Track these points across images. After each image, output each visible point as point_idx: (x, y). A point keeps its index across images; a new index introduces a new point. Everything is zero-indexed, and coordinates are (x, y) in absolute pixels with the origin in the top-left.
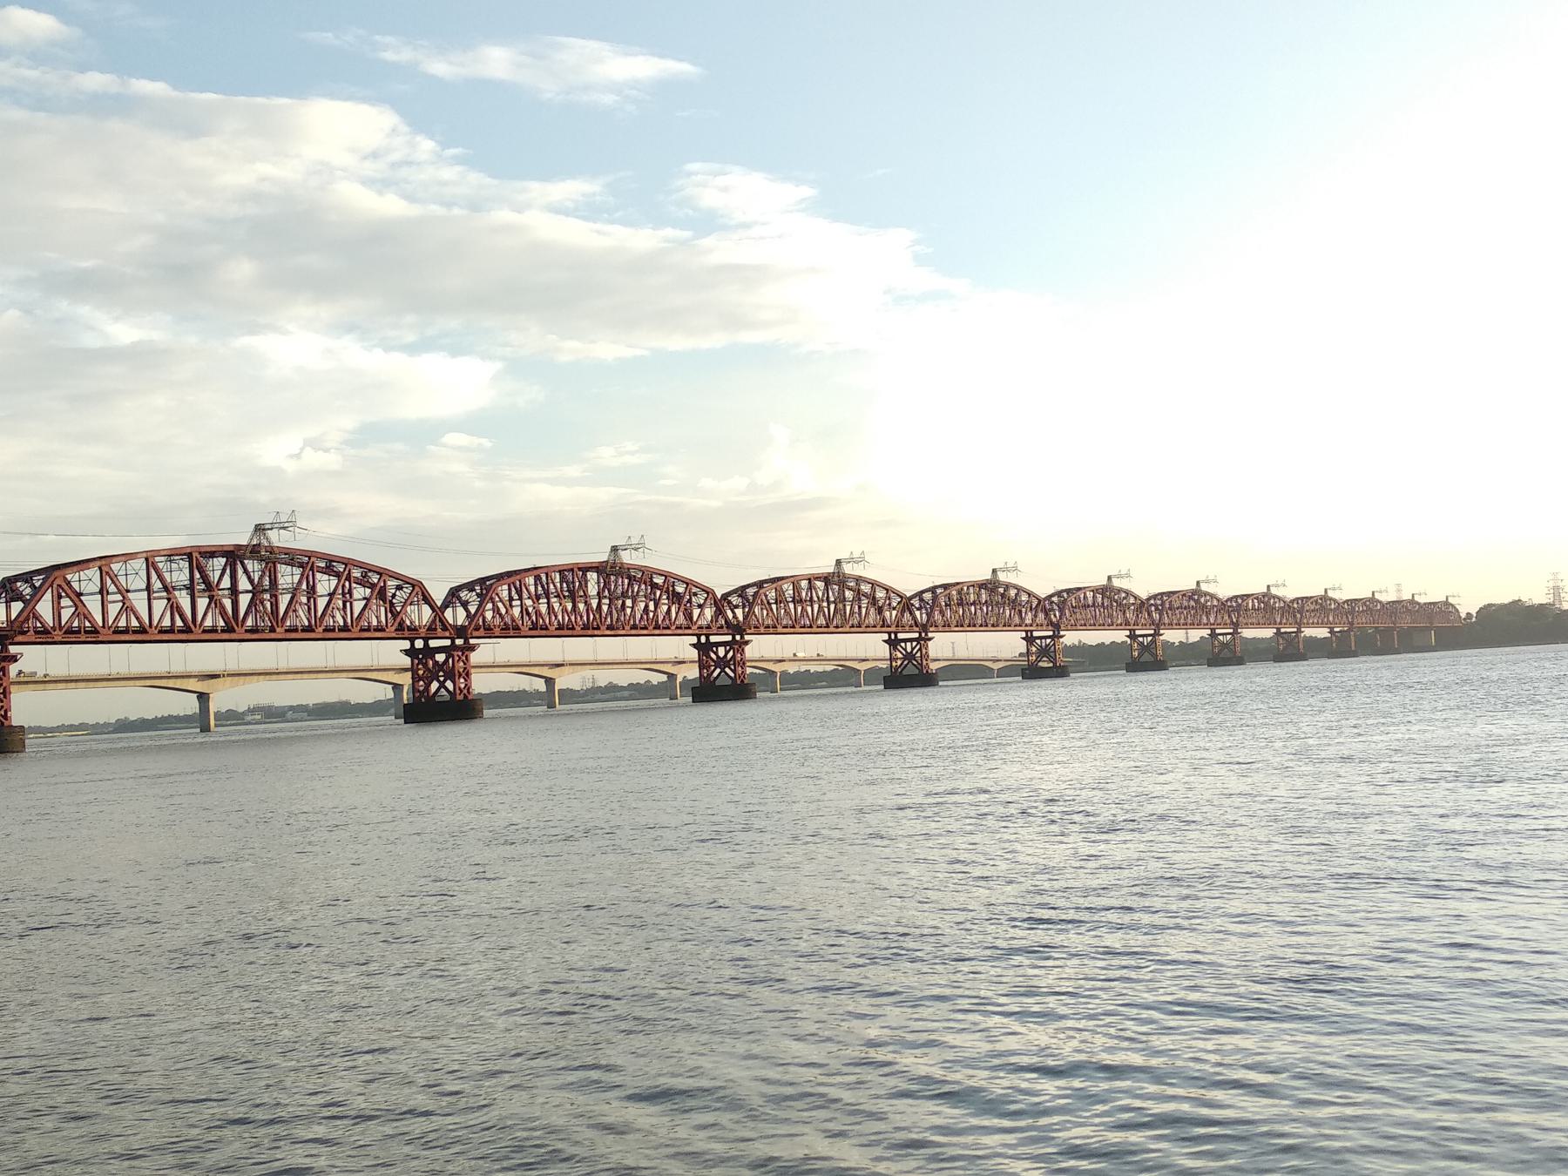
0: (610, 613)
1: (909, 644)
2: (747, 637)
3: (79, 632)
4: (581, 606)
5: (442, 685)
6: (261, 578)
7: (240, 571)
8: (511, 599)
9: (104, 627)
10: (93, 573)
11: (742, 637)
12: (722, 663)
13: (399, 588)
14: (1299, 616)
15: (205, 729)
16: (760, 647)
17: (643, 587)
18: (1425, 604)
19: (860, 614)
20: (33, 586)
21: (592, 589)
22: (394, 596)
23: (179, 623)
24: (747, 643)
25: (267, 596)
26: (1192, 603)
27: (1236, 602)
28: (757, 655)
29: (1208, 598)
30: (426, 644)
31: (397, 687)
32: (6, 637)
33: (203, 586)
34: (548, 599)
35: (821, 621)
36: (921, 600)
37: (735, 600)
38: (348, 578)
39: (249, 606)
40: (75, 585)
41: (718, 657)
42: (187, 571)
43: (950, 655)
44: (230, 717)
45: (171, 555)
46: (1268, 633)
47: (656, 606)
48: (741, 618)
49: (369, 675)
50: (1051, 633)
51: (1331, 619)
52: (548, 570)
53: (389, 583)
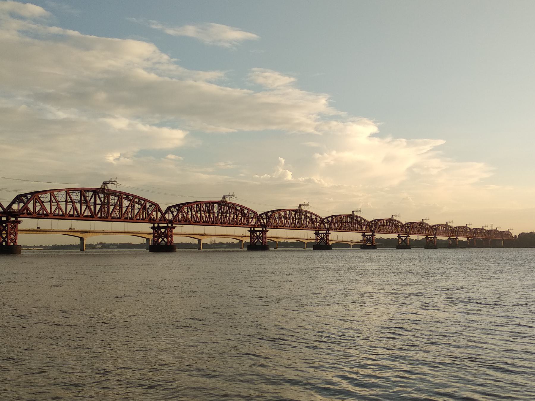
0: (221, 218)
1: (322, 235)
2: (267, 229)
3: (42, 215)
4: (212, 215)
5: (163, 239)
6: (104, 200)
7: (97, 197)
8: (188, 212)
9: (50, 213)
10: (48, 195)
11: (266, 229)
12: (258, 237)
13: (150, 206)
14: (457, 233)
15: (82, 250)
16: (272, 233)
17: (233, 210)
18: (501, 231)
19: (306, 223)
20: (27, 198)
21: (216, 210)
22: (149, 208)
23: (76, 213)
24: (267, 231)
25: (106, 206)
26: (420, 226)
27: (436, 227)
28: (270, 236)
29: (426, 225)
30: (158, 225)
31: (148, 239)
32: (17, 215)
33: (84, 202)
34: (201, 212)
35: (293, 225)
36: (328, 220)
37: (264, 216)
38: (134, 202)
39: (99, 209)
40: (42, 199)
42: (79, 196)
43: (336, 239)
44: (91, 246)
45: (75, 190)
46: (446, 238)
47: (237, 217)
48: (266, 223)
49: (138, 235)
50: (371, 234)
51: (468, 234)
52: (201, 203)
53: (147, 204)
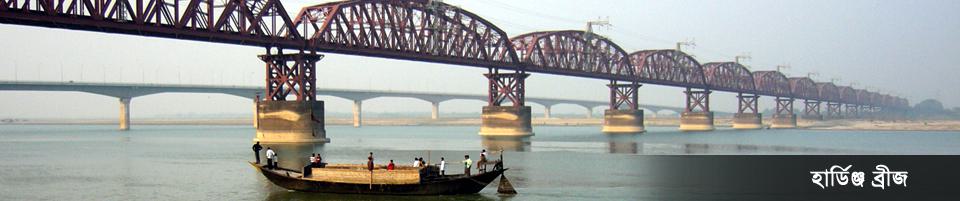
24: (527, 76)
41: (509, 86)
